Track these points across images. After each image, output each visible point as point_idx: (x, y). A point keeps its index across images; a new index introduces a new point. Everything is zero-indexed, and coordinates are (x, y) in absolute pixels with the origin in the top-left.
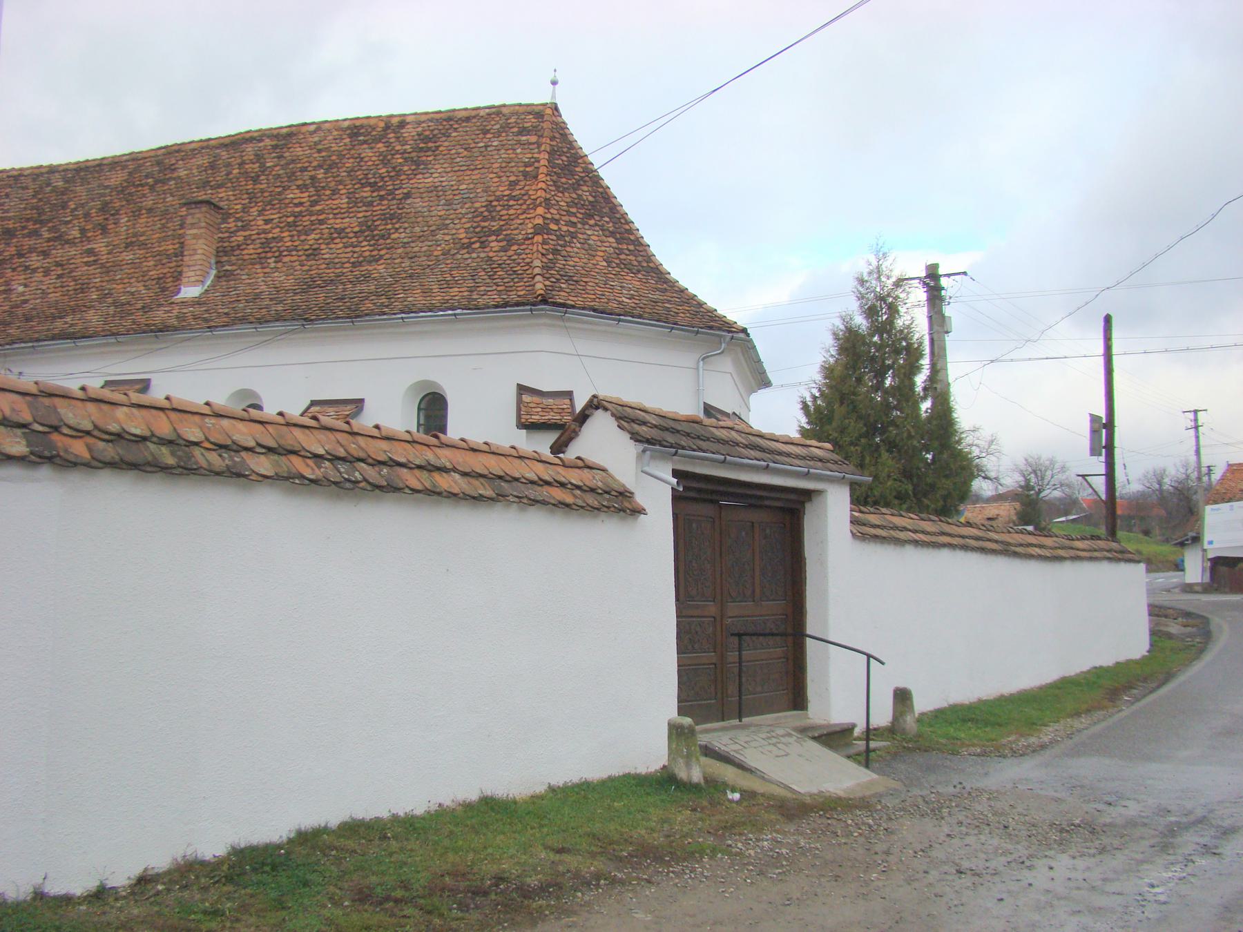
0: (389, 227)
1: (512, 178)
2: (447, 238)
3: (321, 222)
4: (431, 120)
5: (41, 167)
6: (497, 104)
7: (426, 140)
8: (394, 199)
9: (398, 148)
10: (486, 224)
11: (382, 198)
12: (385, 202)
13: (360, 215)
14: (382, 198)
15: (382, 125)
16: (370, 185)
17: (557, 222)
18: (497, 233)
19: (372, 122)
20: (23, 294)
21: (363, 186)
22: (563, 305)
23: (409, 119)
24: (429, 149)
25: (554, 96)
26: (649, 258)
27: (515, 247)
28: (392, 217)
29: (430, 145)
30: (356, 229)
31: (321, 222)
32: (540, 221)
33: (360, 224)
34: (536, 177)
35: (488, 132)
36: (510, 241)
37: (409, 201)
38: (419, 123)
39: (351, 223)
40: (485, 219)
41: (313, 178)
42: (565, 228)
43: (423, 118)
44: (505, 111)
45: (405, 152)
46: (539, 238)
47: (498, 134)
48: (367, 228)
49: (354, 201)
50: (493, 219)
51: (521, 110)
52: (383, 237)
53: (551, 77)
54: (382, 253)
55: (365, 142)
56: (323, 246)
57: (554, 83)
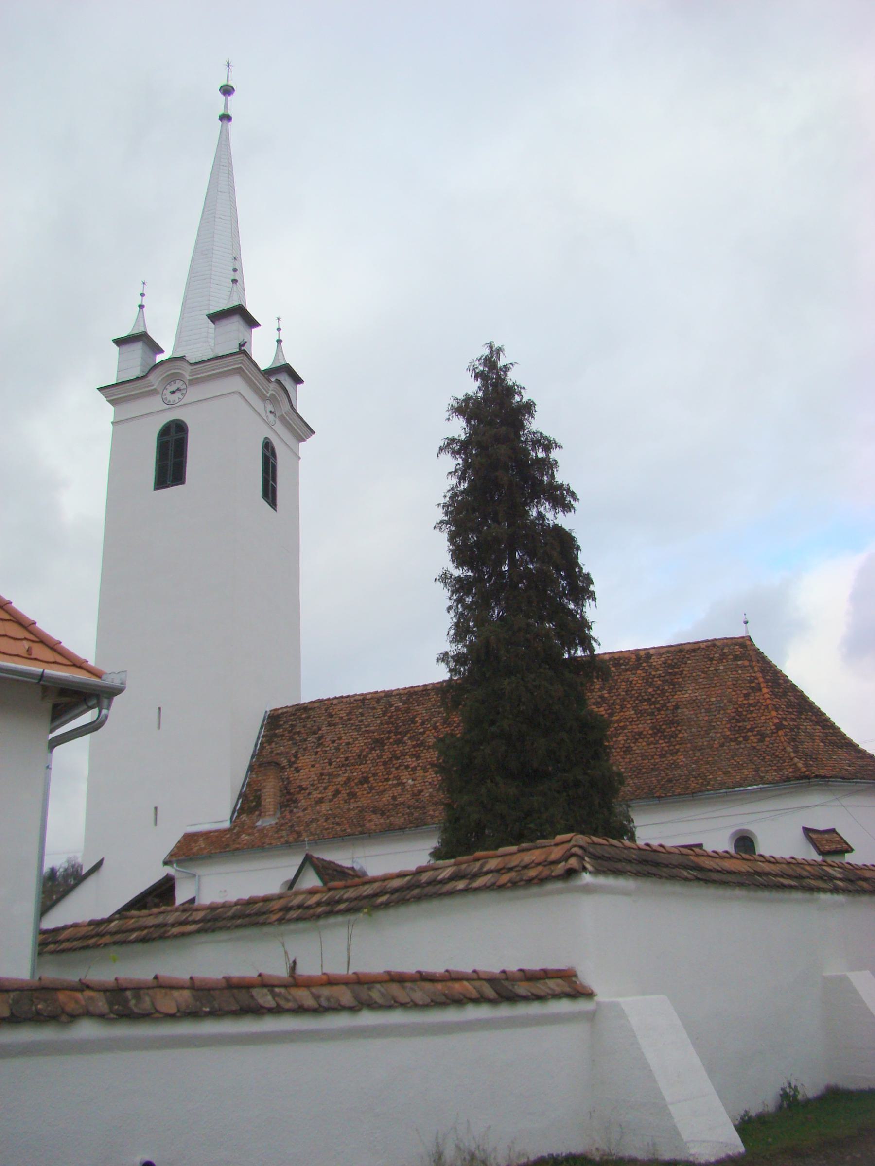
0: (673, 729)
1: (745, 692)
2: (719, 735)
3: (624, 728)
4: (668, 652)
5: (376, 692)
6: (710, 639)
7: (672, 666)
8: (667, 709)
9: (653, 673)
10: (740, 724)
11: (659, 710)
12: (662, 712)
13: (649, 722)
14: (659, 710)
15: (634, 657)
16: (645, 700)
17: (785, 719)
18: (751, 730)
19: (626, 655)
20: (414, 785)
21: (641, 701)
22: (825, 777)
23: (652, 652)
24: (676, 673)
25: (747, 632)
26: (843, 736)
27: (767, 739)
28: (672, 723)
29: (676, 670)
30: (651, 732)
31: (624, 728)
32: (777, 721)
33: (651, 728)
34: (760, 690)
35: (711, 659)
36: (762, 737)
37: (679, 711)
38: (661, 655)
39: (645, 727)
40: (738, 721)
41: (601, 697)
42: (791, 723)
43: (662, 651)
44: (717, 643)
45: (660, 676)
46: (780, 733)
47: (721, 660)
48: (657, 731)
49: (640, 713)
50: (744, 721)
51: (729, 642)
52: (672, 736)
53: (742, 619)
54: (677, 747)
55: (627, 670)
56: (632, 745)
57: (746, 623)
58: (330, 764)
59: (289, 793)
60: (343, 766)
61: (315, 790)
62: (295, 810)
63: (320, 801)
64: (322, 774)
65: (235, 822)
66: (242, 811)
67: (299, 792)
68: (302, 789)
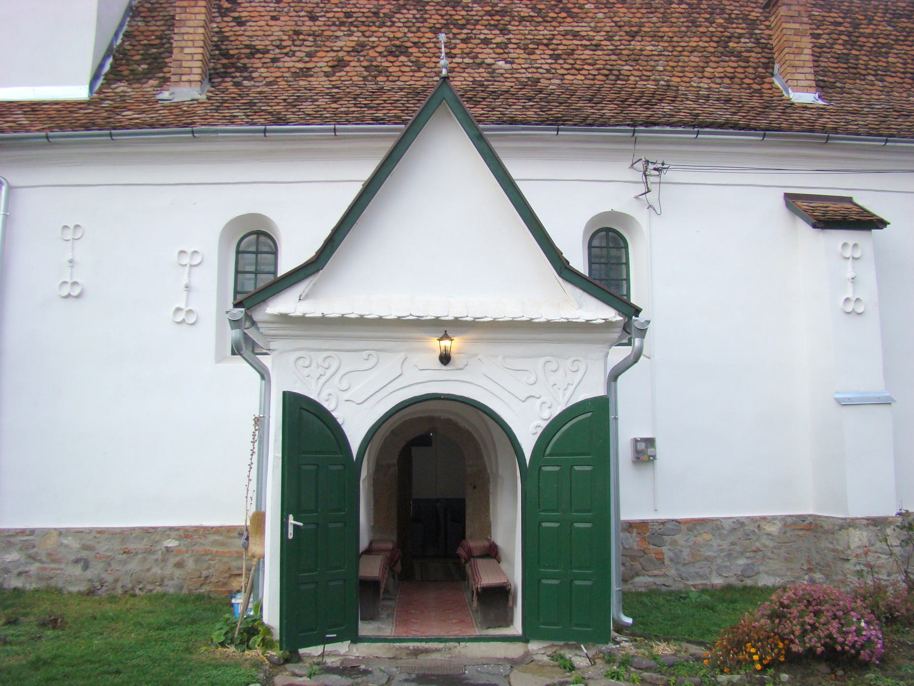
58: (313, 18)
59: (226, 55)
60: (343, 24)
61: (286, 54)
62: (246, 83)
63: (305, 73)
64: (298, 33)
65: (100, 92)
66: (115, 76)
67: (251, 56)
68: (254, 51)
